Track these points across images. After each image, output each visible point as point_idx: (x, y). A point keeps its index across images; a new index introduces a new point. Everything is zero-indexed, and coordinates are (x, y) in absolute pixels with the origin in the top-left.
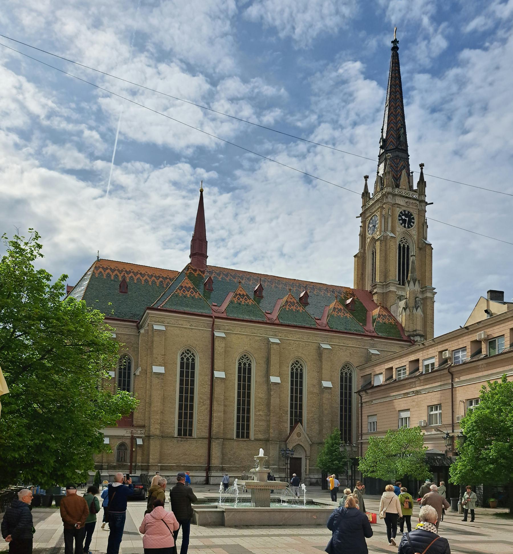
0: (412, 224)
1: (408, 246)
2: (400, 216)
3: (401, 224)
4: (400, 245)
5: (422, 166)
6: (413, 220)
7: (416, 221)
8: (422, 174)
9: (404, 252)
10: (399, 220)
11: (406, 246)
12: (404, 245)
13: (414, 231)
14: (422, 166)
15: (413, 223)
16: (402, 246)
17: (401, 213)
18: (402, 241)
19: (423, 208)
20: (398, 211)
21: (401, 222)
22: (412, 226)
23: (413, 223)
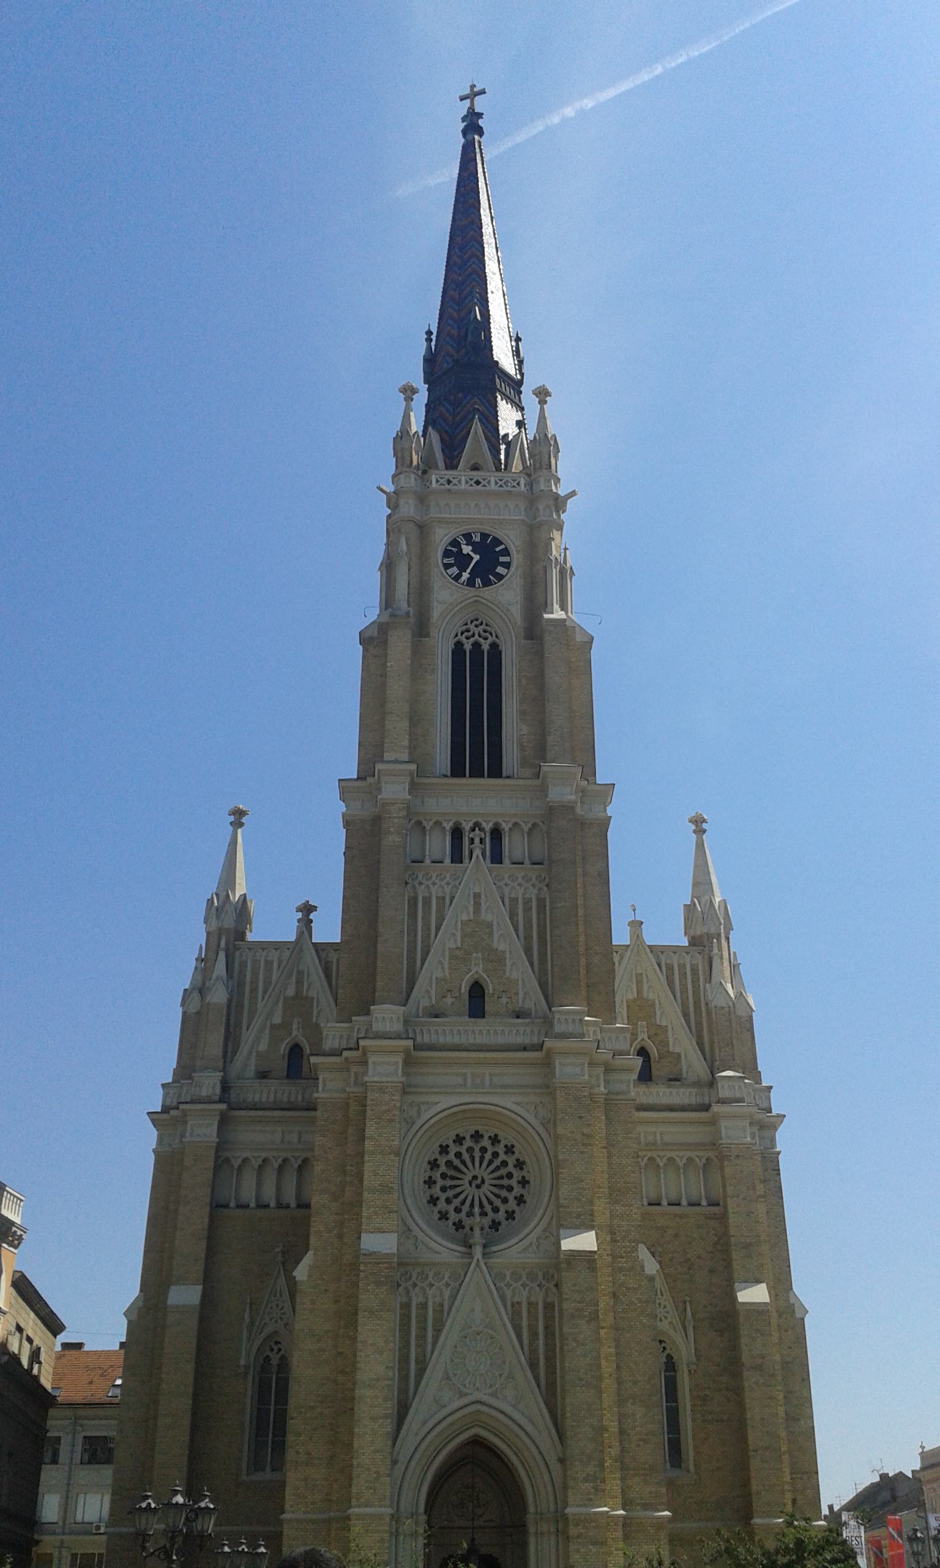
0: (500, 570)
1: (494, 646)
2: (447, 554)
3: (457, 578)
4: (459, 645)
6: (502, 559)
7: (517, 559)
8: (542, 418)
10: (447, 566)
11: (486, 647)
12: (477, 646)
13: (507, 594)
15: (507, 565)
16: (468, 647)
17: (455, 543)
18: (468, 631)
21: (454, 570)
22: (500, 577)
23: (507, 565)
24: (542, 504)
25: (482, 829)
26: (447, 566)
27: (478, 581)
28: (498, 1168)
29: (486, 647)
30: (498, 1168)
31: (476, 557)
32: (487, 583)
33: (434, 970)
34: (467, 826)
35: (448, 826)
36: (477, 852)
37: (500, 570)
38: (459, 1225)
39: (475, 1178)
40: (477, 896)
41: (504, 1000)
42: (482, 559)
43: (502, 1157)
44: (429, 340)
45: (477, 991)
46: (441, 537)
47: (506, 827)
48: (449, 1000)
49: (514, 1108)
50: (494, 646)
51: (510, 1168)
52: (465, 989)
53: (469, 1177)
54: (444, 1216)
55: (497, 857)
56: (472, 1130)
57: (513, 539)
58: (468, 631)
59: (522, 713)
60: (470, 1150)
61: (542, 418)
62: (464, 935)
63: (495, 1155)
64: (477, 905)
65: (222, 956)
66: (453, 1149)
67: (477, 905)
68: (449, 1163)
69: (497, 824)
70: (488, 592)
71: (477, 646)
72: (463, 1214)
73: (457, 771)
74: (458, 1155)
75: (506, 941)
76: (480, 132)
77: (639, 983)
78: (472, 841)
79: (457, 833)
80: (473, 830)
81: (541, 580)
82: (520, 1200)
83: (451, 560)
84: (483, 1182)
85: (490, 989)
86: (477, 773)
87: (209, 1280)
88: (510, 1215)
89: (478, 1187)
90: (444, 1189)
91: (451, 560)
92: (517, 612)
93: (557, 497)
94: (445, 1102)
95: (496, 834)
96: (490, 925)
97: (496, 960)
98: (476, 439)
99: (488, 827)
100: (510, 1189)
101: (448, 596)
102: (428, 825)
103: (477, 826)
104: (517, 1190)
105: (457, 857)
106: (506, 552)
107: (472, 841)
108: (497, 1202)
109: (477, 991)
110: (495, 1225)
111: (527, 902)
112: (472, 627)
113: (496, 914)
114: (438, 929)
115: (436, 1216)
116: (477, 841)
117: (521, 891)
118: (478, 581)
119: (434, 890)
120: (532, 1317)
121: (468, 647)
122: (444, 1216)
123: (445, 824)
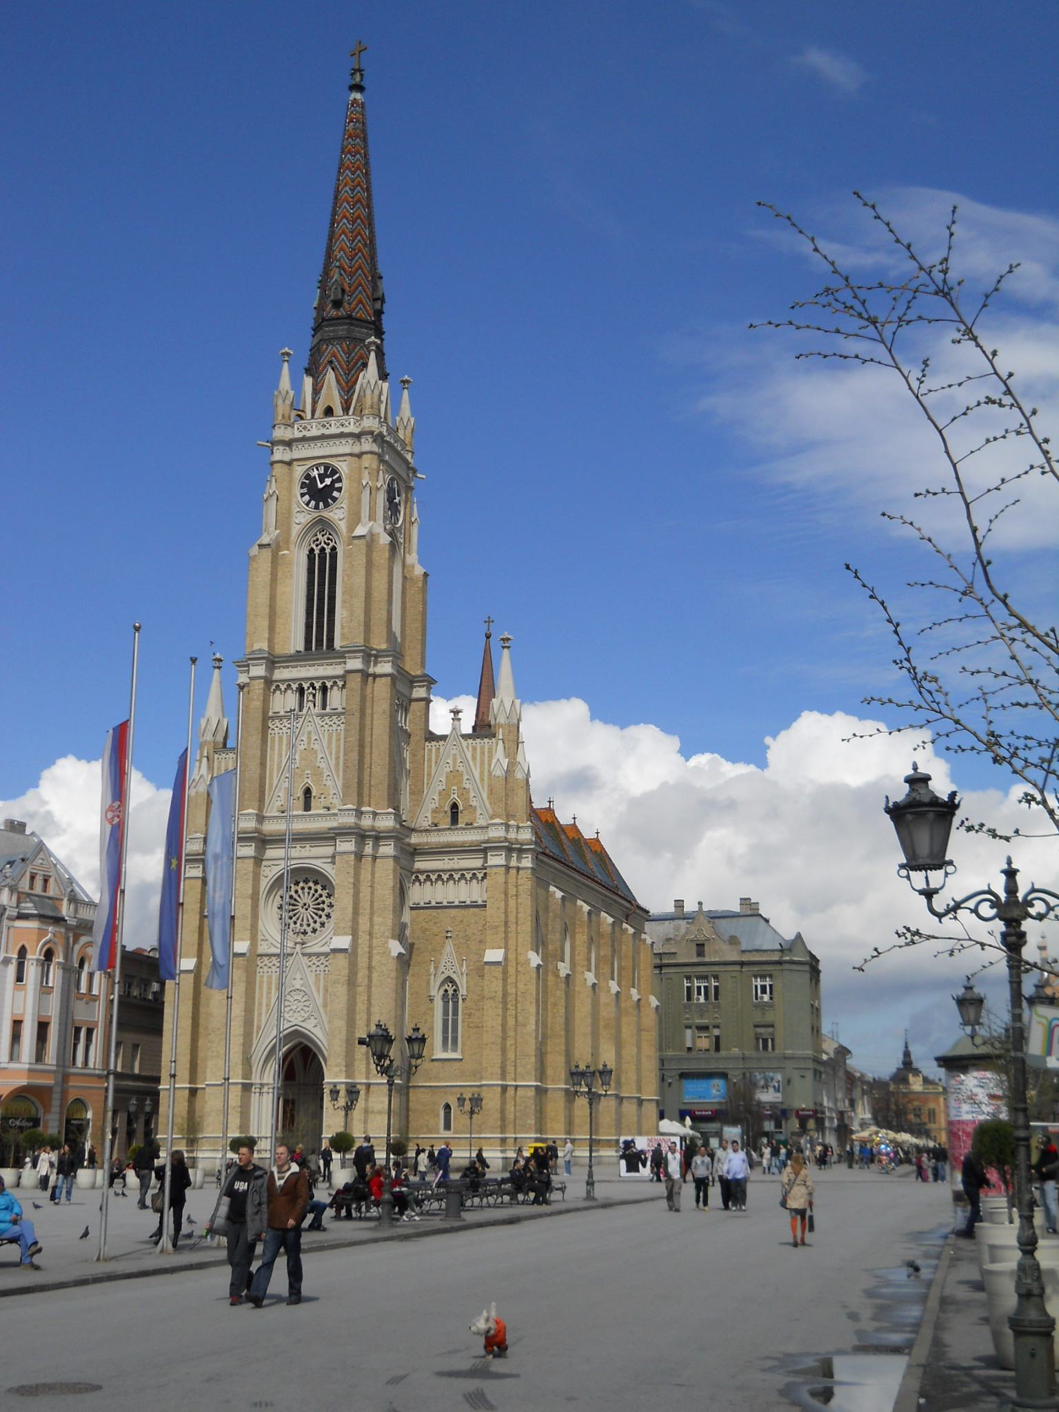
0: (335, 494)
2: (303, 485)
3: (307, 504)
4: (312, 551)
7: (345, 484)
10: (302, 495)
11: (328, 551)
13: (337, 514)
15: (339, 490)
16: (317, 552)
20: (299, 471)
21: (307, 498)
22: (335, 499)
23: (339, 490)
25: (314, 688)
27: (321, 504)
29: (328, 551)
31: (320, 486)
32: (327, 505)
34: (305, 686)
35: (294, 686)
40: (310, 733)
45: (308, 792)
47: (329, 684)
50: (334, 549)
52: (300, 793)
53: (301, 904)
57: (343, 467)
59: (344, 601)
60: (303, 888)
62: (302, 759)
64: (309, 738)
65: (205, 760)
67: (309, 738)
68: (291, 897)
69: (324, 684)
70: (326, 514)
71: (323, 549)
74: (296, 892)
77: (455, 760)
79: (301, 691)
83: (305, 490)
87: (200, 955)
88: (323, 925)
91: (305, 490)
95: (324, 689)
96: (316, 752)
97: (317, 773)
98: (329, 387)
99: (317, 685)
100: (323, 910)
105: (301, 707)
108: (316, 918)
109: (308, 792)
110: (314, 931)
112: (319, 536)
118: (321, 504)
121: (317, 552)
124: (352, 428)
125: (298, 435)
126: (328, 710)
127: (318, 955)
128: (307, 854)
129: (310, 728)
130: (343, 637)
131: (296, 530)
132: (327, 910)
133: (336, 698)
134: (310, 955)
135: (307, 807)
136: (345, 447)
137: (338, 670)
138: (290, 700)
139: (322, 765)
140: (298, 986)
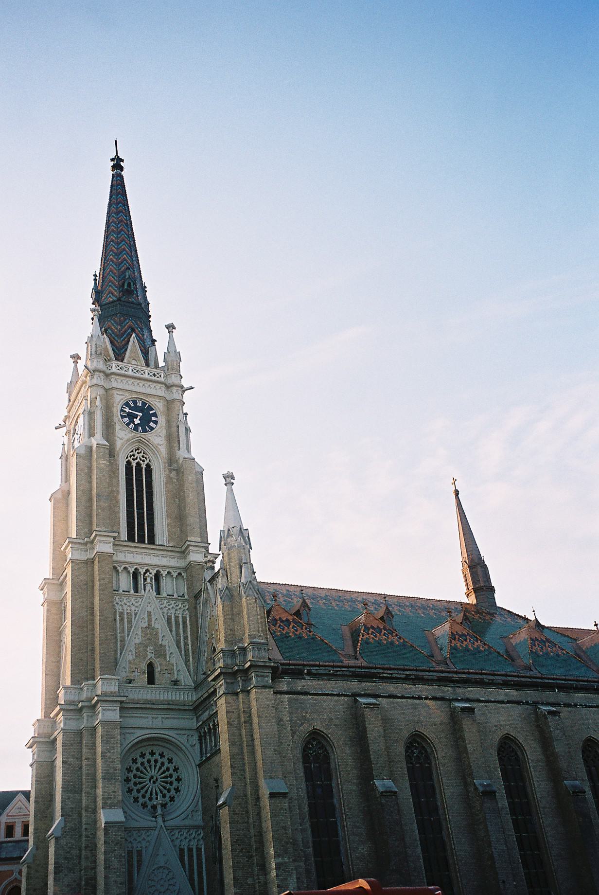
0: (151, 424)
1: (148, 466)
4: (129, 463)
5: (170, 327)
6: (153, 418)
7: (162, 420)
8: (171, 340)
9: (139, 479)
10: (123, 417)
11: (144, 466)
12: (138, 464)
13: (157, 437)
14: (170, 327)
16: (134, 465)
18: (134, 455)
19: (175, 394)
21: (127, 420)
23: (156, 423)
24: (175, 389)
26: (123, 417)
28: (164, 772)
29: (144, 466)
30: (164, 772)
32: (145, 431)
33: (129, 656)
34: (142, 571)
35: (132, 570)
36: (148, 587)
37: (151, 424)
38: (144, 805)
39: (152, 777)
41: (166, 675)
42: (141, 415)
43: (166, 765)
44: (95, 280)
45: (151, 667)
46: (119, 400)
47: (164, 573)
48: (136, 674)
49: (177, 737)
50: (148, 466)
51: (171, 771)
52: (144, 667)
53: (149, 777)
54: (136, 800)
55: (158, 592)
56: (149, 749)
57: (159, 406)
58: (134, 455)
61: (171, 340)
63: (163, 764)
64: (149, 619)
66: (140, 760)
67: (149, 619)
69: (158, 572)
70: (144, 435)
72: (147, 799)
73: (131, 538)
74: (142, 764)
75: (168, 640)
76: (122, 169)
78: (145, 580)
79: (136, 574)
80: (145, 573)
81: (177, 434)
82: (177, 790)
84: (157, 780)
85: (157, 669)
86: (141, 540)
88: (172, 799)
89: (154, 782)
90: (135, 784)
92: (163, 450)
93: (182, 387)
94: (139, 734)
95: (157, 576)
97: (160, 652)
101: (123, 435)
102: (120, 569)
103: (147, 571)
104: (175, 784)
105: (136, 591)
106: (155, 415)
107: (145, 580)
109: (151, 667)
111: (177, 618)
112: (136, 453)
113: (160, 625)
114: (129, 632)
115: (132, 800)
116: (148, 580)
117: (173, 611)
118: (140, 429)
119: (125, 607)
120: (191, 856)
121: (134, 465)
122: (136, 800)
123: (129, 569)
124: (162, 379)
125: (114, 370)
126: (165, 595)
127: (180, 828)
128: (160, 725)
129: (149, 609)
130: (171, 538)
131: (119, 444)
132: (175, 784)
133: (167, 585)
134: (171, 830)
135: (151, 680)
136: (161, 391)
137: (173, 562)
138: (125, 582)
139: (165, 643)
140: (162, 864)
